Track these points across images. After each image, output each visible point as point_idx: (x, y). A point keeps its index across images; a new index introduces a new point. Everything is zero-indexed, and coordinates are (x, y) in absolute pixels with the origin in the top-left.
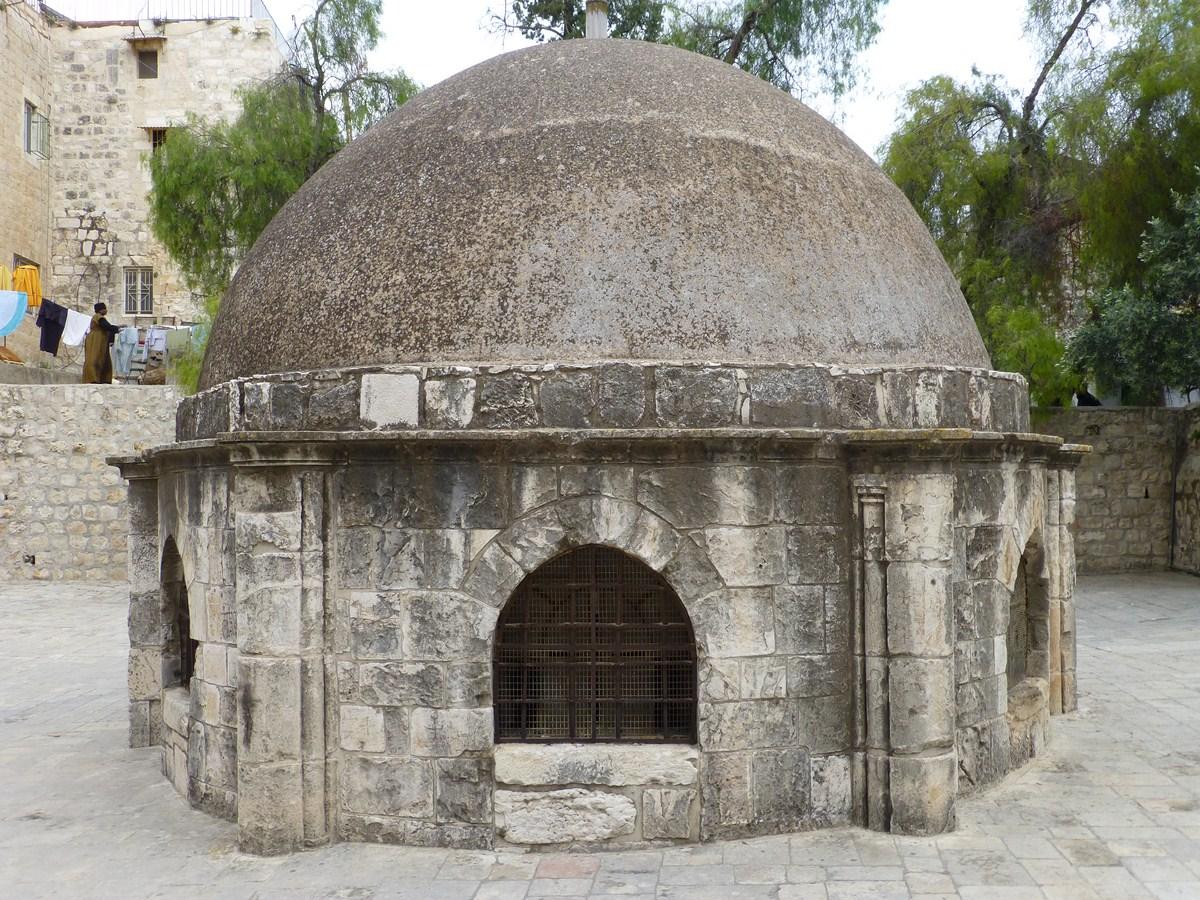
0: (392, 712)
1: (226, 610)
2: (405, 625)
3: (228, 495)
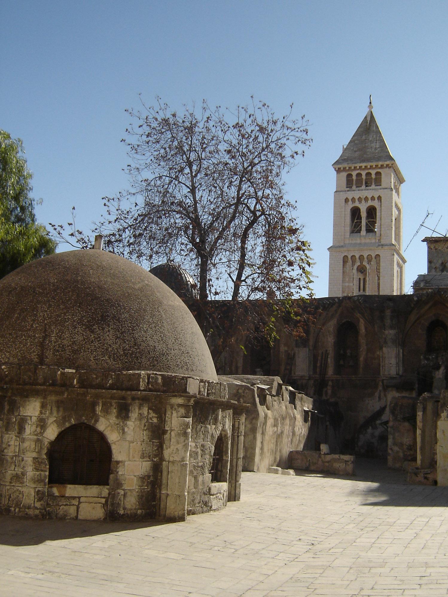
0: (196, 478)
1: (144, 449)
2: (199, 450)
3: (148, 411)
